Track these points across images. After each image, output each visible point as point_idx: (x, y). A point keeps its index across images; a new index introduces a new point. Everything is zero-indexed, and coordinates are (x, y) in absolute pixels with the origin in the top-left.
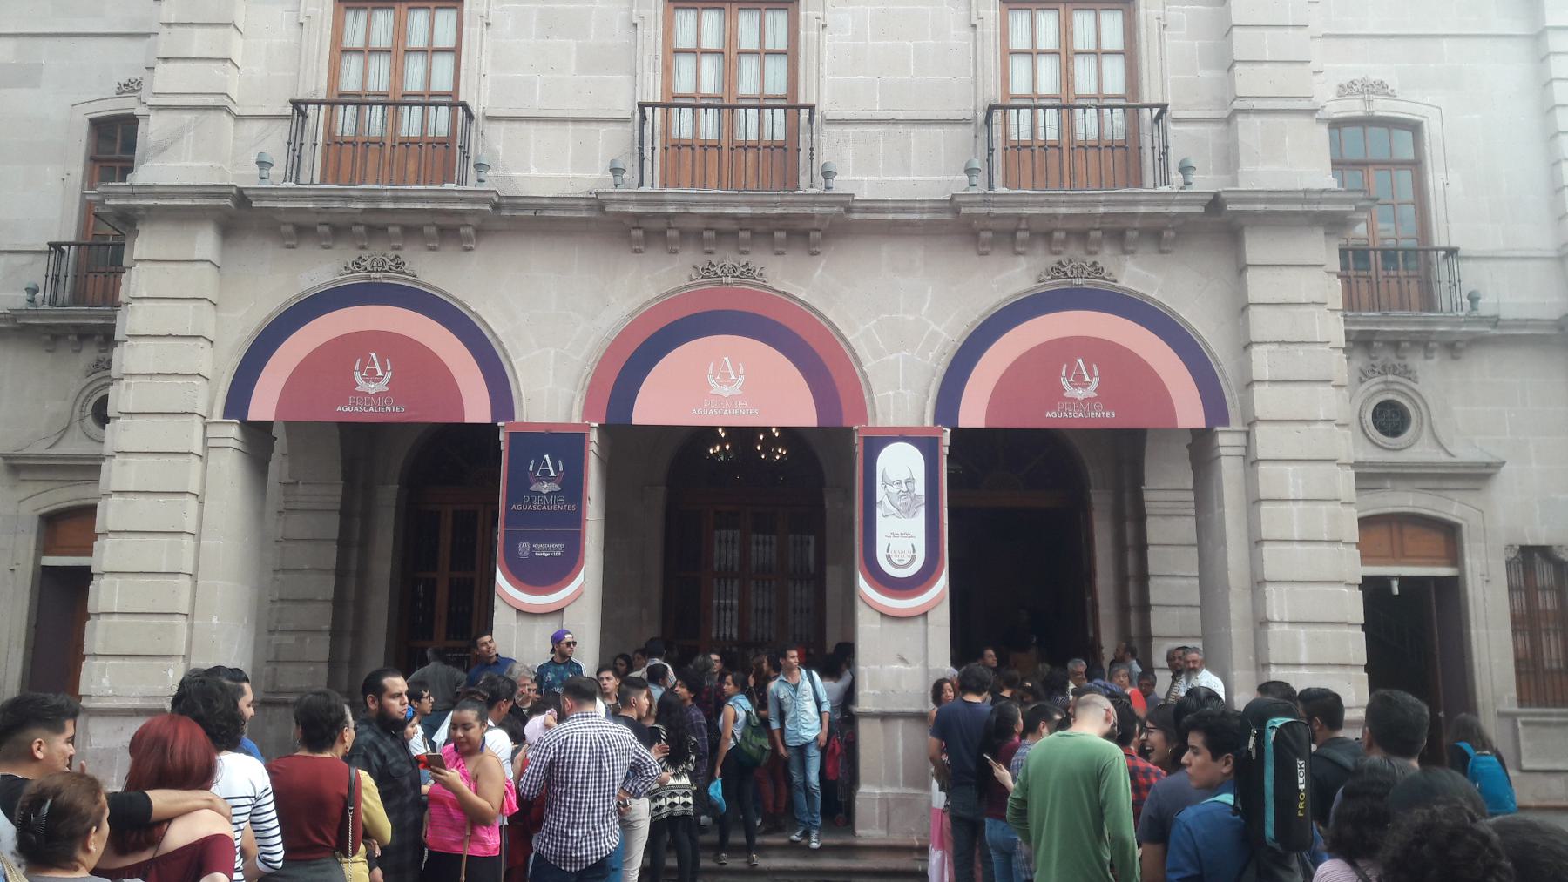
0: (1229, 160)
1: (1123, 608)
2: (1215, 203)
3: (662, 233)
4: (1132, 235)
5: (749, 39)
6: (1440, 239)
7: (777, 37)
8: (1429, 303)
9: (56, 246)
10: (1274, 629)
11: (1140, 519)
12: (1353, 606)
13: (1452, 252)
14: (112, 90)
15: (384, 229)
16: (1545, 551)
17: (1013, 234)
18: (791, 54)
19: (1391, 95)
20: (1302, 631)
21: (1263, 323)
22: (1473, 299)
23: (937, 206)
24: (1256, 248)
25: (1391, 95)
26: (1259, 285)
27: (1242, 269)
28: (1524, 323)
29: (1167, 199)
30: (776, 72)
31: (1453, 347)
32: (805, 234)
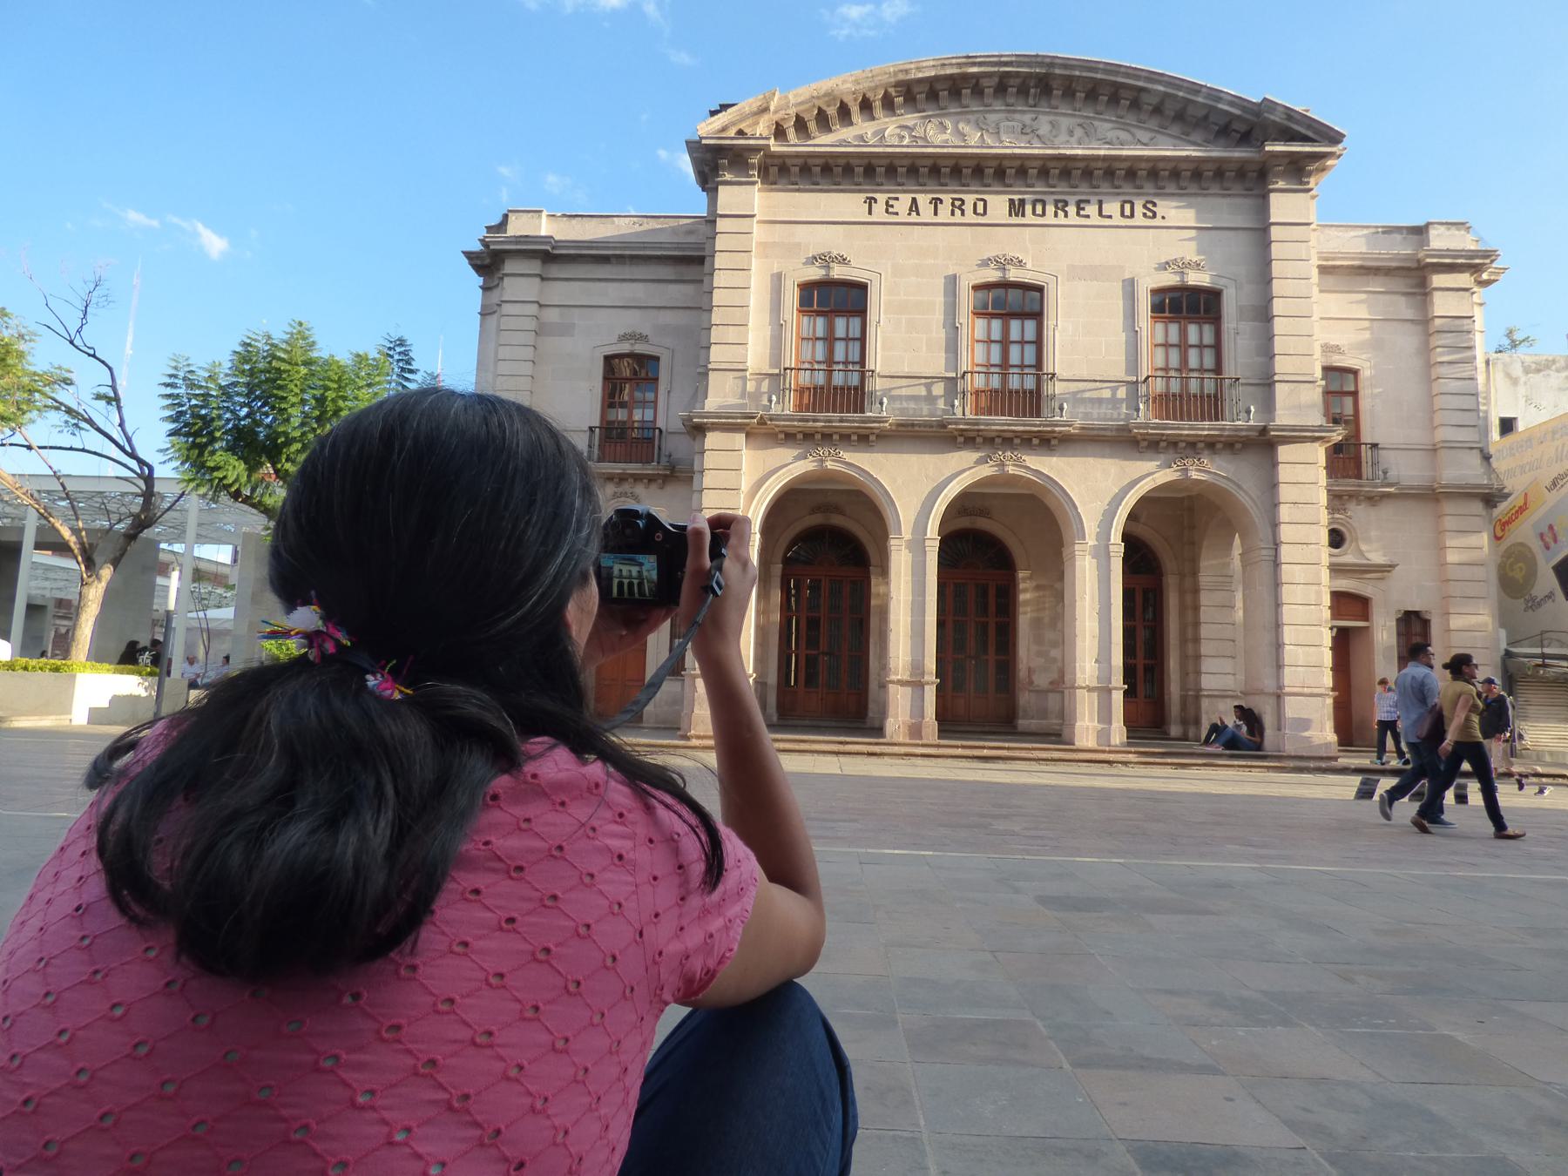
0: (1268, 405)
1: (1183, 641)
2: (1264, 430)
3: (973, 439)
4: (1219, 446)
5: (1015, 334)
6: (1367, 436)
7: (1030, 334)
8: (1359, 476)
9: (591, 429)
10: (1287, 648)
11: (1196, 591)
12: (1327, 638)
13: (1374, 446)
14: (614, 339)
15: (831, 435)
16: (1417, 614)
17: (1157, 443)
18: (1039, 343)
19: (1342, 353)
20: (1300, 650)
21: (1285, 493)
22: (1385, 473)
23: (1120, 429)
24: (1284, 452)
25: (1342, 353)
26: (1284, 473)
27: (1274, 464)
28: (1412, 488)
29: (1237, 429)
30: (1030, 351)
31: (1373, 500)
32: (1048, 441)
